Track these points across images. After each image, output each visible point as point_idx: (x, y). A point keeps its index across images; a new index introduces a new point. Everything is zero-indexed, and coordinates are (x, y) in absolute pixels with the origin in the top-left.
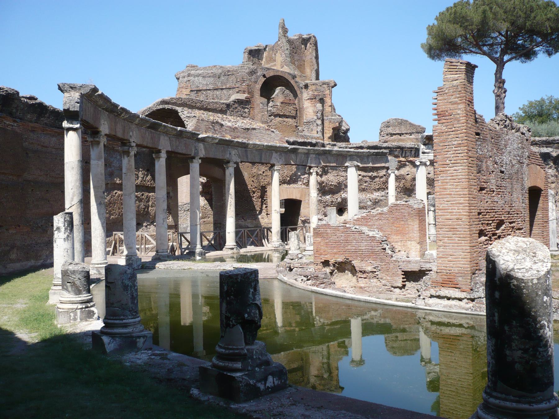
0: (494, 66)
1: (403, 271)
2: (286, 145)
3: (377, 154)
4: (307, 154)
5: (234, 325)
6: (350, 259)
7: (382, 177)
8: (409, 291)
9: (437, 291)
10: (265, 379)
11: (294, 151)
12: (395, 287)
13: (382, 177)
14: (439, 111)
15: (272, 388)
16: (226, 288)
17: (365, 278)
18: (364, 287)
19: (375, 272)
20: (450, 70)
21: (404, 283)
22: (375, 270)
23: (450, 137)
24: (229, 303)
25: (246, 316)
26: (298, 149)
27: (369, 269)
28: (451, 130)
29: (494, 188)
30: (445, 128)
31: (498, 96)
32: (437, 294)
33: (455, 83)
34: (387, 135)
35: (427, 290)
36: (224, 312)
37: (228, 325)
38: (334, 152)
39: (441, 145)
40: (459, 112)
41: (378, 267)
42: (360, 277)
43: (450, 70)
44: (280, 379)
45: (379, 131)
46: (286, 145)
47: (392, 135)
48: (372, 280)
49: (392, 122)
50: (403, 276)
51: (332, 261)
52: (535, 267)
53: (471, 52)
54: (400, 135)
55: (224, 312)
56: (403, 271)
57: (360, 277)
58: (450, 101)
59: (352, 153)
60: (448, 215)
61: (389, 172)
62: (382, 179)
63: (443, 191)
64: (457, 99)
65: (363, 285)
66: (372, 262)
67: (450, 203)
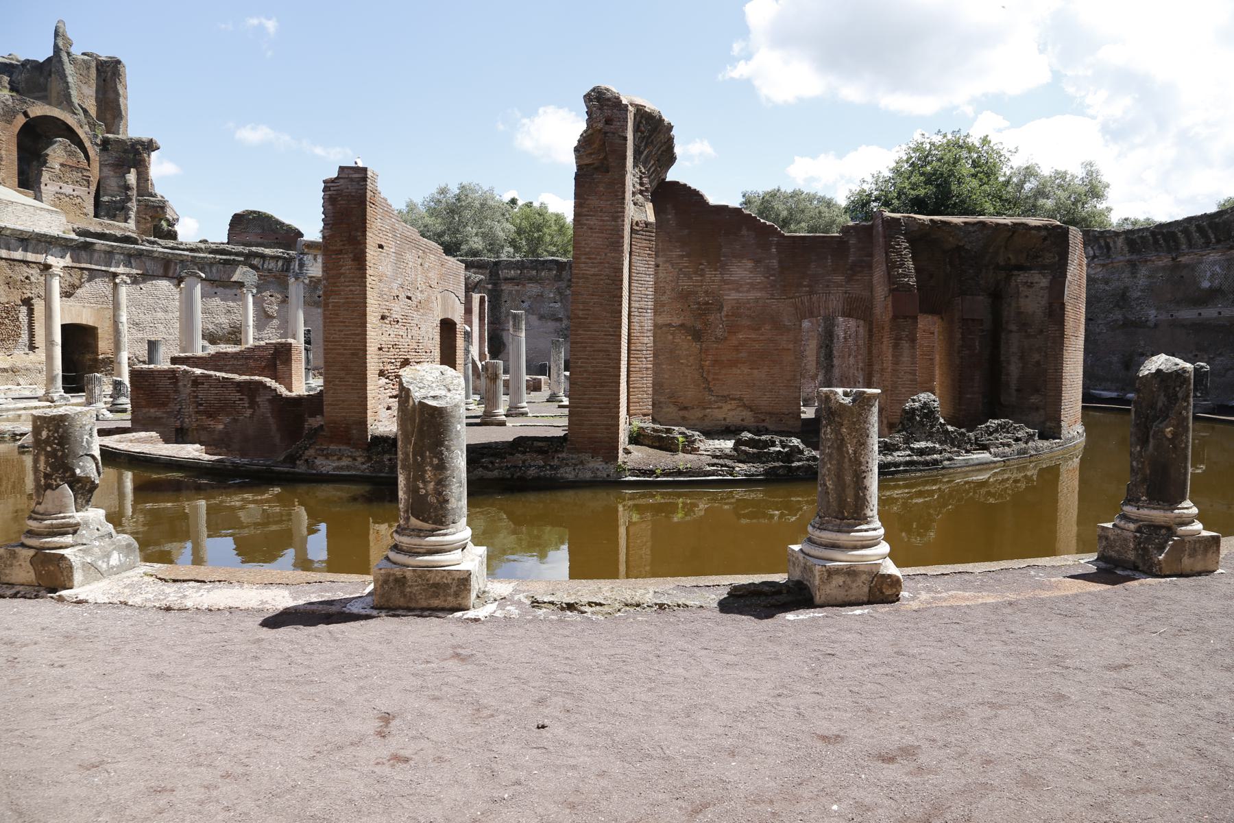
2: (73, 236)
3: (226, 262)
4: (110, 253)
5: (58, 486)
10: (108, 556)
11: (87, 246)
15: (118, 567)
16: (44, 434)
24: (48, 455)
25: (78, 471)
26: (93, 244)
29: (399, 317)
36: (42, 468)
37: (48, 487)
44: (127, 556)
46: (73, 236)
52: (449, 394)
55: (42, 468)
61: (245, 290)
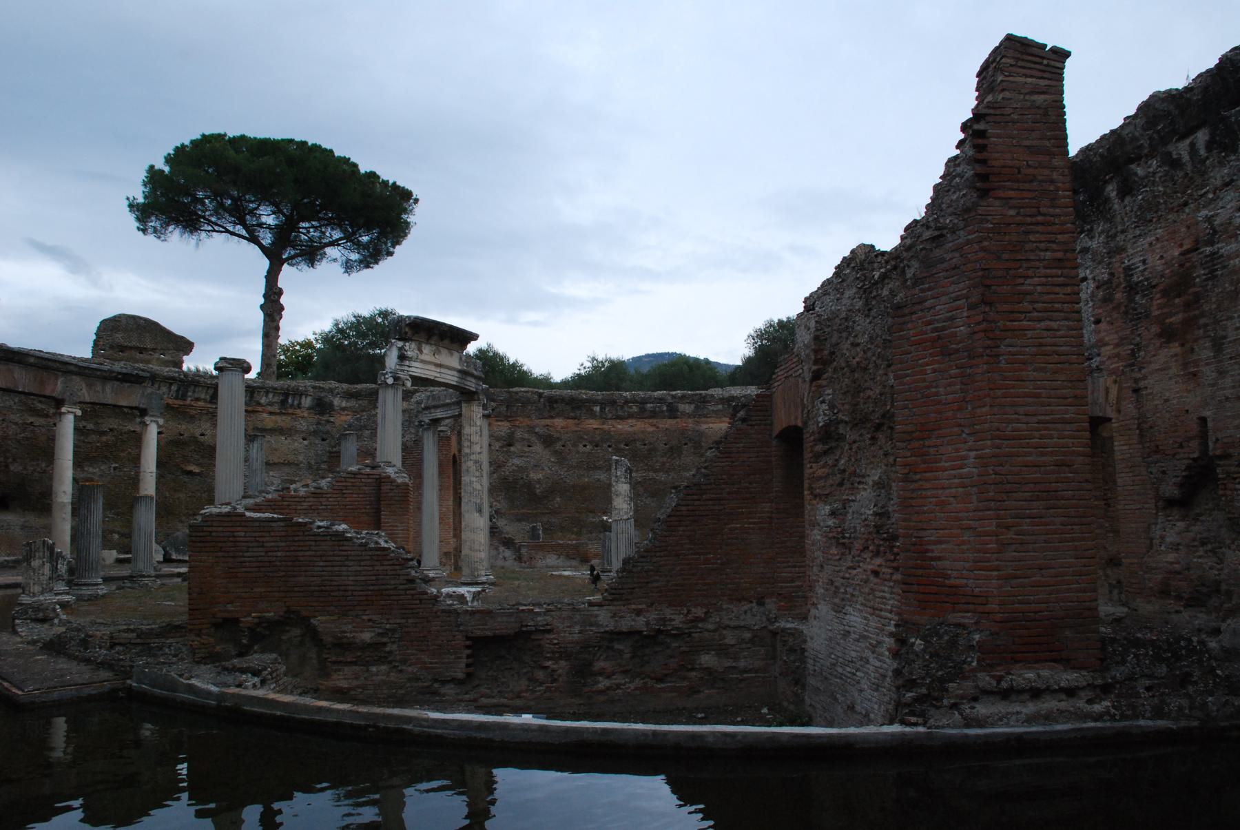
0: (265, 263)
1: (468, 638)
6: (304, 613)
7: (104, 433)
8: (483, 689)
9: (999, 680)
12: (444, 682)
13: (104, 433)
14: (996, 163)
17: (351, 663)
18: (349, 689)
19: (385, 644)
20: (1020, 63)
21: (471, 669)
22: (384, 640)
23: (1032, 238)
27: (367, 636)
28: (1034, 220)
30: (1012, 212)
31: (266, 315)
32: (1004, 685)
33: (1040, 99)
34: (112, 347)
35: (965, 678)
38: (32, 360)
39: (1005, 256)
40: (1055, 176)
41: (393, 631)
42: (334, 663)
43: (1020, 63)
45: (94, 337)
47: (123, 349)
48: (374, 669)
49: (124, 322)
50: (469, 652)
51: (247, 620)
53: (227, 231)
54: (141, 350)
56: (468, 638)
57: (334, 663)
58: (1027, 143)
59: (72, 368)
60: (1030, 454)
61: (147, 419)
62: (104, 438)
63: (1013, 387)
64: (1047, 143)
65: (344, 684)
66: (374, 617)
67: (1035, 419)
